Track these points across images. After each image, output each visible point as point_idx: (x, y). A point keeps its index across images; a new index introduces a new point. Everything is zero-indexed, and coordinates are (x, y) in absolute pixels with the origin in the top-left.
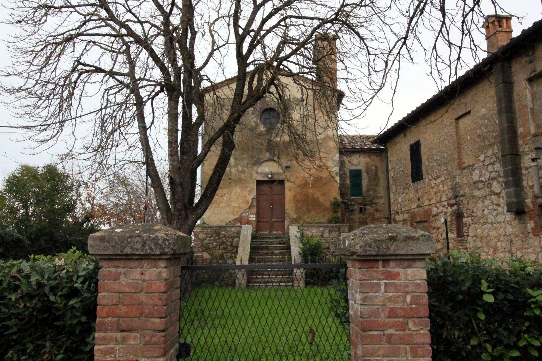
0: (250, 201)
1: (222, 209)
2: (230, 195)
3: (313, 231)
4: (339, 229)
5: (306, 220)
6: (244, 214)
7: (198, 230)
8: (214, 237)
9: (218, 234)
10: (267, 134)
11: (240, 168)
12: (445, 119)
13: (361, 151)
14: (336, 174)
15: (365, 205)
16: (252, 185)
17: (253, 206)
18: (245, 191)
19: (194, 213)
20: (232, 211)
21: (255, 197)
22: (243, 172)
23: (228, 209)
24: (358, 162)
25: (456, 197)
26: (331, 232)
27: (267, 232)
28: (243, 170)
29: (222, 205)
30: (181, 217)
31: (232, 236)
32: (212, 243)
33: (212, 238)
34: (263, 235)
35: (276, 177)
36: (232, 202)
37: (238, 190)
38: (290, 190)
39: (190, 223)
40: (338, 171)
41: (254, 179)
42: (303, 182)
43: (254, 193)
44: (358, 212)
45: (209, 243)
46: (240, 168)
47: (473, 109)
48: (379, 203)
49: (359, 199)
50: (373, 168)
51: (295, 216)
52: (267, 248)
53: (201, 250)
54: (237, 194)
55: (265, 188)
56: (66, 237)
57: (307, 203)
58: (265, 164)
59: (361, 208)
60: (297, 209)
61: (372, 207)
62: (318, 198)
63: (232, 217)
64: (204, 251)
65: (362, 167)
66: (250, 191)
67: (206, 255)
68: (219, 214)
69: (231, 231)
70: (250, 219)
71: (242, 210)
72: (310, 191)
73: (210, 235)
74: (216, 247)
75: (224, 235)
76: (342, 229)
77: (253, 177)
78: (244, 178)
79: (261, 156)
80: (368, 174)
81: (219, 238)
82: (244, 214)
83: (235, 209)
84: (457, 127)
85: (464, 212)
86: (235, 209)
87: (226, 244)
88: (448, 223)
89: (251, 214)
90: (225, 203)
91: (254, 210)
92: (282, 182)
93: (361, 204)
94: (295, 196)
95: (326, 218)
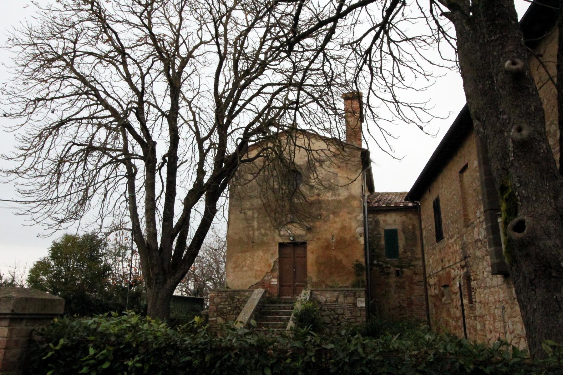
0: (272, 265)
2: (253, 258)
3: (328, 295)
4: (355, 293)
5: (329, 284)
6: (266, 278)
7: (214, 295)
8: (229, 302)
9: (232, 299)
11: (263, 231)
12: (451, 173)
13: (397, 209)
14: (361, 235)
15: (402, 267)
16: (274, 248)
17: (275, 269)
19: (173, 277)
21: (277, 260)
22: (265, 235)
23: (250, 273)
24: (391, 221)
25: (466, 257)
26: (346, 297)
27: (290, 297)
28: (265, 233)
29: (245, 269)
30: (158, 281)
32: (226, 308)
33: (227, 303)
34: (285, 299)
35: (298, 240)
37: (261, 253)
38: (312, 252)
39: (167, 286)
41: (276, 242)
42: (325, 244)
43: (277, 256)
44: (394, 276)
46: (263, 231)
47: (469, 161)
48: (417, 265)
49: (395, 261)
50: (411, 227)
52: (277, 314)
53: (215, 314)
54: (260, 257)
55: (288, 251)
56: (102, 301)
57: (330, 265)
59: (398, 271)
60: (319, 271)
61: (410, 269)
62: (341, 260)
63: (254, 281)
64: (218, 316)
65: (397, 226)
66: (272, 254)
67: (220, 320)
68: (242, 278)
69: (245, 296)
70: (272, 283)
71: (264, 274)
72: (333, 253)
73: (224, 300)
74: (230, 312)
75: (238, 299)
76: (357, 294)
77: (276, 240)
80: (404, 233)
81: (233, 303)
82: (266, 278)
83: (257, 273)
84: (461, 181)
85: (472, 274)
86: (257, 273)
88: (462, 288)
89: (274, 278)
90: (248, 266)
91: (277, 274)
92: (304, 244)
93: (397, 267)
95: (350, 282)
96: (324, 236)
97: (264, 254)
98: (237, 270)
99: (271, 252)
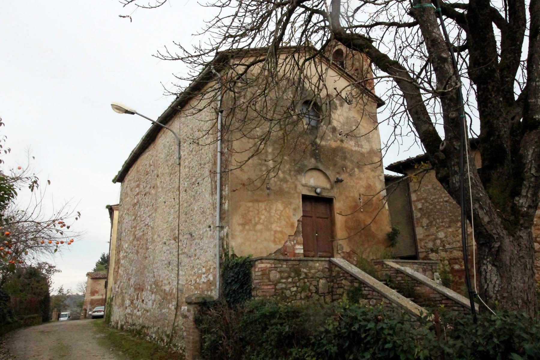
1: (259, 234)
2: (269, 212)
6: (288, 243)
7: (269, 265)
8: (293, 278)
9: (298, 273)
10: (310, 134)
16: (297, 201)
18: (289, 208)
20: (272, 238)
21: (301, 219)
22: (284, 180)
23: (267, 235)
29: (259, 227)
31: (317, 275)
32: (289, 289)
33: (290, 280)
36: (272, 224)
37: (280, 206)
40: (386, 194)
41: (299, 193)
42: (353, 204)
45: (286, 289)
51: (348, 250)
54: (279, 212)
58: (310, 173)
66: (295, 209)
68: (255, 241)
70: (297, 252)
73: (286, 274)
74: (295, 295)
75: (306, 274)
78: (287, 190)
79: (306, 162)
81: (299, 280)
82: (288, 243)
83: (277, 235)
86: (277, 235)
87: (310, 290)
89: (298, 243)
90: (263, 224)
91: (300, 238)
92: (329, 202)
94: (346, 222)
96: (352, 195)
97: (285, 208)
98: (247, 227)
99: (293, 206)
